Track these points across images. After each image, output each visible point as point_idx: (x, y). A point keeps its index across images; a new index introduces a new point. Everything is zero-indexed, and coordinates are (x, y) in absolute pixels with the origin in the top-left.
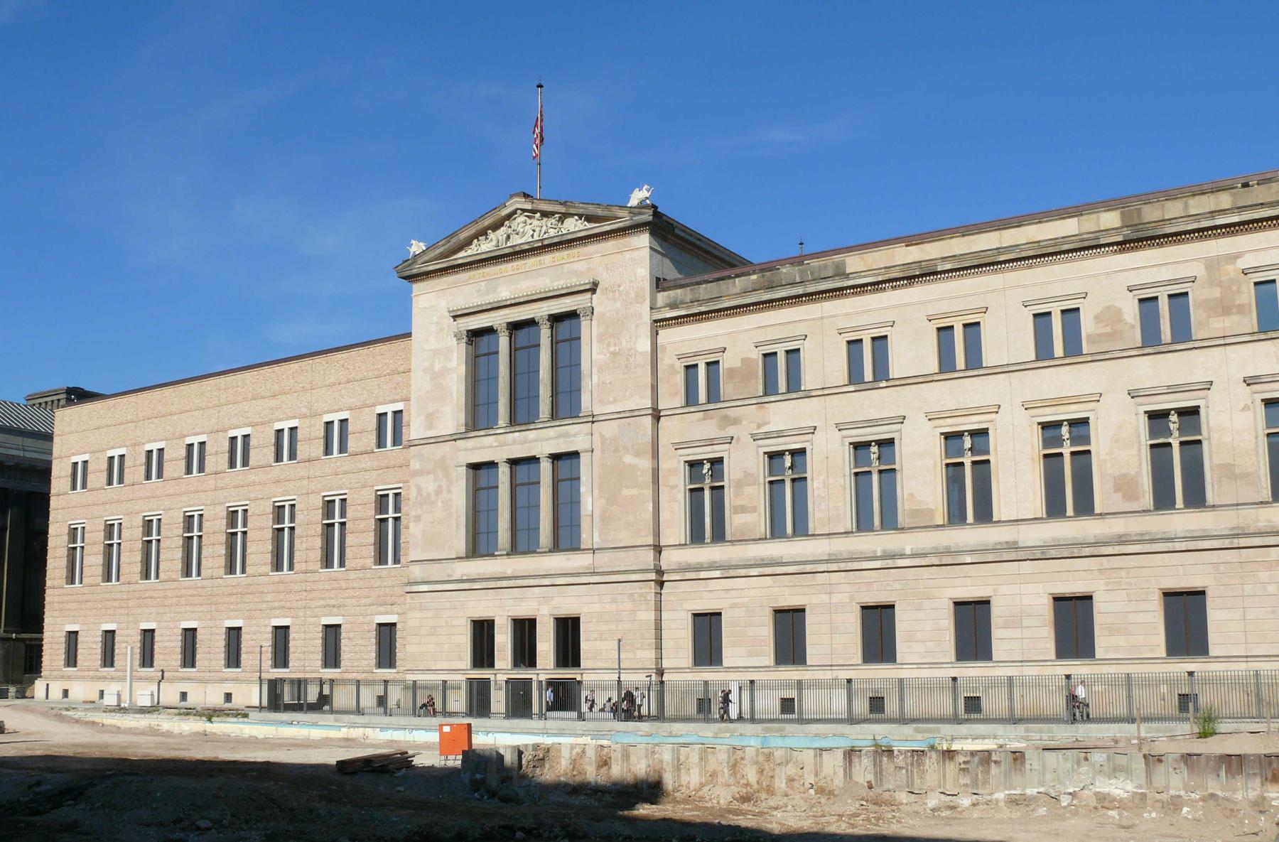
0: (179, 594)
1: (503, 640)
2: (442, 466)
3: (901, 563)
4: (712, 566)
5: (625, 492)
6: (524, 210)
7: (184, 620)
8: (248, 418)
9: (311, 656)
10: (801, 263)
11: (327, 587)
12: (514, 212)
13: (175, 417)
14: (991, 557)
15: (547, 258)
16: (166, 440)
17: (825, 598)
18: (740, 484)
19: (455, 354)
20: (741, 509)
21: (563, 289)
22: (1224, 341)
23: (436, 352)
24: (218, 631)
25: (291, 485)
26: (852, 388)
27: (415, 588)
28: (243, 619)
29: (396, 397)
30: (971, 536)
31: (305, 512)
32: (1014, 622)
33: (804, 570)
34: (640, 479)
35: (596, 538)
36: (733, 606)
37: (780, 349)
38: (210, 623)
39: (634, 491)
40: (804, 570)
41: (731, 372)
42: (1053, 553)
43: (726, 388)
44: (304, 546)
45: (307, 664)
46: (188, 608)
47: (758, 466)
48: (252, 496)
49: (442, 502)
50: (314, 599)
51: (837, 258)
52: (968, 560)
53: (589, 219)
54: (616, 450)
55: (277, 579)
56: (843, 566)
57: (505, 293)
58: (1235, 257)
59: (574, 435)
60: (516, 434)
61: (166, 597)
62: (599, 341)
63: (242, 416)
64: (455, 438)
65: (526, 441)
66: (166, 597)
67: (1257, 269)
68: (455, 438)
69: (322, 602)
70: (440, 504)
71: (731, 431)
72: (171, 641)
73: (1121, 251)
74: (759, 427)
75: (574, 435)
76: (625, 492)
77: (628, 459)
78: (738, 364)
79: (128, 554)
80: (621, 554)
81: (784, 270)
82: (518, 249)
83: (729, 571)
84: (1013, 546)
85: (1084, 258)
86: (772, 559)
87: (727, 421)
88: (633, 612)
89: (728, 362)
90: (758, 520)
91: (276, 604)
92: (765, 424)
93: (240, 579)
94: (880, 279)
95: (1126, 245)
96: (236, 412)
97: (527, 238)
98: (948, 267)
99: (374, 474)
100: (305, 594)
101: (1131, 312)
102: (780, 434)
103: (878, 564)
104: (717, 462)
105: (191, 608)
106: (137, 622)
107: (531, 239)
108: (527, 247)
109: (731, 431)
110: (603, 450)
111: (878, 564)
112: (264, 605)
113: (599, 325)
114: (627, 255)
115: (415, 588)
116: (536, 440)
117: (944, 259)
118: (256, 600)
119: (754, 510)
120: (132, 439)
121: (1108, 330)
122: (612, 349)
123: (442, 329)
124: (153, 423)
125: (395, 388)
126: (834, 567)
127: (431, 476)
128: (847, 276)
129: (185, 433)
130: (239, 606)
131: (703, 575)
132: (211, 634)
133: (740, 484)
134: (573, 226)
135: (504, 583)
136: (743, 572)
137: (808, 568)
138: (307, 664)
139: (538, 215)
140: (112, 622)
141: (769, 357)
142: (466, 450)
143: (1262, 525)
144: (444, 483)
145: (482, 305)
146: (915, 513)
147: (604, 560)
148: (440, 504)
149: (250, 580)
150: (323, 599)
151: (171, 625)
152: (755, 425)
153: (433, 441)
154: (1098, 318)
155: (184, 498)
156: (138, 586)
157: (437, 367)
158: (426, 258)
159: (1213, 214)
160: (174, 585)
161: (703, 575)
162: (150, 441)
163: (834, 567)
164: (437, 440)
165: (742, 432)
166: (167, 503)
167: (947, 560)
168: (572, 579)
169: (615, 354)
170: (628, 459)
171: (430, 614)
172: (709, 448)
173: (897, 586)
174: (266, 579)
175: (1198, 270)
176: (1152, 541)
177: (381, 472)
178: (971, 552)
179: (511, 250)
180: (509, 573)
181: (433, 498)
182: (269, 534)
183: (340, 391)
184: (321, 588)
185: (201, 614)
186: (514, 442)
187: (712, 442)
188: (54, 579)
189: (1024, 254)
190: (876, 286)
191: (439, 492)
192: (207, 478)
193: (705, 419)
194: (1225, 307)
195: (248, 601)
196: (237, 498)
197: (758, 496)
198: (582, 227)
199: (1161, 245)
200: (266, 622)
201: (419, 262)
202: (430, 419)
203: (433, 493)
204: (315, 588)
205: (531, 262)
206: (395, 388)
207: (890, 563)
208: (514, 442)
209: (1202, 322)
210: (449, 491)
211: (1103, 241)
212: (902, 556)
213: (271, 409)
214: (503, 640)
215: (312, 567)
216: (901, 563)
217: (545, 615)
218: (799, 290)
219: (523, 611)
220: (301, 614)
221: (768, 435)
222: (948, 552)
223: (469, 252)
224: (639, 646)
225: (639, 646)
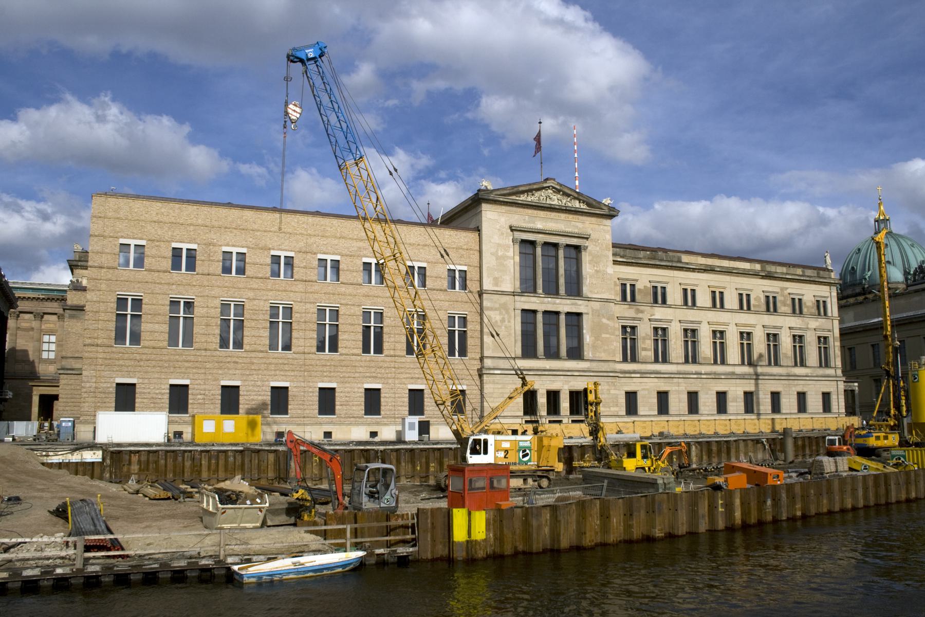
0: (267, 362)
1: (542, 400)
2: (504, 307)
3: (703, 376)
4: (634, 372)
5: (604, 336)
6: (553, 188)
7: (272, 381)
8: (337, 249)
9: (399, 408)
10: (666, 252)
11: (412, 367)
12: (549, 187)
13: (258, 233)
14: (729, 377)
15: (563, 216)
16: (247, 247)
17: (677, 388)
18: (644, 339)
19: (512, 249)
20: (645, 349)
21: (576, 234)
22: (785, 314)
23: (499, 245)
24: (311, 390)
25: (380, 300)
26: (685, 307)
27: (492, 372)
28: (337, 383)
29: (461, 263)
30: (720, 369)
31: (392, 319)
32: (735, 400)
33: (670, 376)
34: (610, 331)
35: (590, 355)
36: (643, 389)
37: (659, 285)
38: (303, 384)
39: (608, 336)
40: (670, 376)
41: (640, 290)
42: (746, 377)
43: (638, 297)
44: (392, 340)
45: (396, 413)
46: (278, 372)
47: (651, 332)
48: (343, 302)
49: (506, 327)
50: (402, 373)
51: (679, 254)
52: (723, 377)
53: (589, 205)
54: (599, 316)
55: (368, 359)
56: (684, 376)
57: (539, 225)
58: (787, 288)
59: (580, 305)
60: (550, 299)
61: (253, 363)
62: (589, 263)
63: (331, 247)
64: (514, 294)
65: (554, 303)
66: (253, 363)
67: (792, 294)
68: (514, 294)
69: (408, 375)
70: (503, 327)
71: (640, 315)
72: (260, 395)
73: (762, 278)
74: (651, 316)
75: (580, 305)
76: (604, 336)
77: (604, 321)
78: (643, 288)
79: (204, 327)
80: (602, 364)
81: (660, 253)
82: (553, 206)
83: (643, 374)
84: (733, 373)
85: (754, 278)
86: (657, 371)
87: (638, 311)
88: (609, 390)
89: (639, 286)
90: (651, 354)
91: (368, 374)
92: (654, 315)
93: (333, 356)
94: (697, 268)
95: (763, 277)
96: (325, 243)
97: (556, 202)
98: (718, 270)
99: (447, 304)
100: (393, 369)
101: (763, 300)
102: (660, 320)
103: (695, 376)
104: (633, 328)
105: (282, 373)
106: (217, 380)
107: (557, 204)
108: (558, 207)
109: (640, 315)
110: (592, 314)
111: (695, 376)
112: (357, 375)
113: (589, 255)
114: (602, 227)
115: (492, 372)
116: (560, 304)
117: (718, 266)
118: (349, 370)
119: (650, 350)
120: (205, 240)
121: (757, 304)
122: (596, 268)
123: (502, 234)
124: (231, 232)
125: (461, 257)
126: (681, 376)
127: (498, 312)
128: (681, 262)
129: (270, 246)
130: (332, 374)
131: (633, 375)
132: (304, 392)
133: (644, 339)
134: (577, 204)
135: (547, 373)
136: (648, 375)
137: (672, 376)
138: (396, 413)
139: (561, 193)
140: (187, 378)
141: (655, 288)
142: (520, 301)
143: (792, 373)
144: (506, 316)
145: (532, 229)
146: (705, 358)
147: (594, 366)
148: (503, 327)
149: (342, 358)
150: (409, 373)
151: (259, 383)
152: (649, 315)
153: (500, 293)
154: (755, 299)
155: (271, 293)
156: (218, 353)
157: (500, 253)
158: (499, 193)
159: (782, 273)
160: (261, 355)
161: (633, 375)
162: (228, 245)
163: (681, 376)
164: (503, 293)
165: (646, 316)
166: (251, 294)
167: (716, 376)
168: (583, 373)
169: (597, 271)
170: (604, 321)
171: (500, 386)
172: (632, 321)
173: (700, 385)
174: (359, 358)
175: (778, 290)
176: (771, 375)
177: (452, 303)
178: (724, 374)
179: (549, 206)
180: (548, 367)
181: (499, 323)
182: (360, 329)
183: (419, 249)
184: (408, 367)
185: (293, 377)
186: (549, 303)
187: (634, 319)
188: (97, 338)
189: (740, 272)
190: (693, 270)
191: (503, 321)
192: (296, 283)
193: (629, 308)
194: (785, 305)
195: (342, 371)
196: (327, 301)
197: (650, 344)
198: (584, 207)
199: (771, 279)
200: (359, 385)
201: (494, 193)
202: (496, 281)
203: (499, 322)
204: (402, 366)
205: (553, 215)
206: (461, 257)
207: (699, 376)
208: (549, 303)
209: (782, 308)
210: (509, 322)
211: (760, 274)
212: (701, 374)
213: (360, 248)
214: (542, 400)
215: (398, 353)
216: (703, 376)
217: (566, 390)
218: (670, 264)
219: (554, 387)
220: (390, 381)
221: (656, 320)
222: (715, 374)
223: (529, 199)
224: (611, 405)
225: (611, 405)
